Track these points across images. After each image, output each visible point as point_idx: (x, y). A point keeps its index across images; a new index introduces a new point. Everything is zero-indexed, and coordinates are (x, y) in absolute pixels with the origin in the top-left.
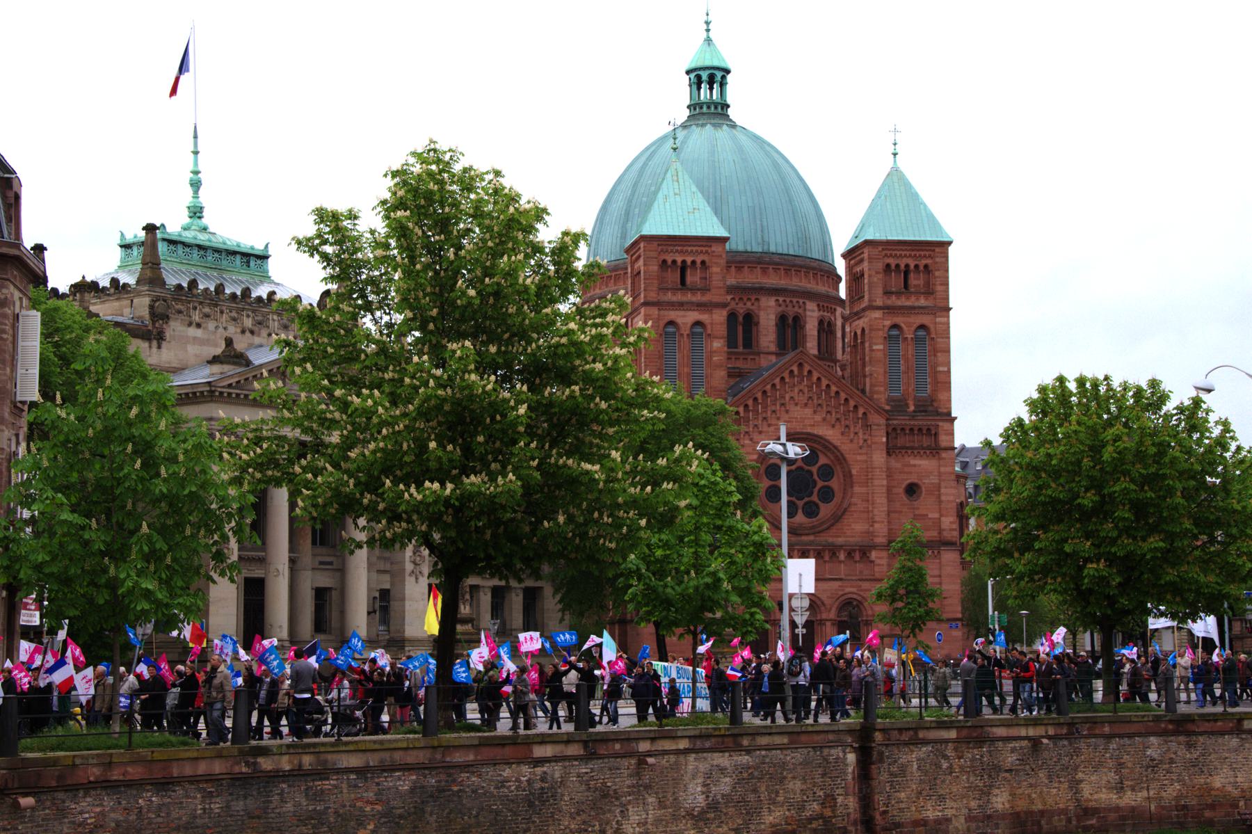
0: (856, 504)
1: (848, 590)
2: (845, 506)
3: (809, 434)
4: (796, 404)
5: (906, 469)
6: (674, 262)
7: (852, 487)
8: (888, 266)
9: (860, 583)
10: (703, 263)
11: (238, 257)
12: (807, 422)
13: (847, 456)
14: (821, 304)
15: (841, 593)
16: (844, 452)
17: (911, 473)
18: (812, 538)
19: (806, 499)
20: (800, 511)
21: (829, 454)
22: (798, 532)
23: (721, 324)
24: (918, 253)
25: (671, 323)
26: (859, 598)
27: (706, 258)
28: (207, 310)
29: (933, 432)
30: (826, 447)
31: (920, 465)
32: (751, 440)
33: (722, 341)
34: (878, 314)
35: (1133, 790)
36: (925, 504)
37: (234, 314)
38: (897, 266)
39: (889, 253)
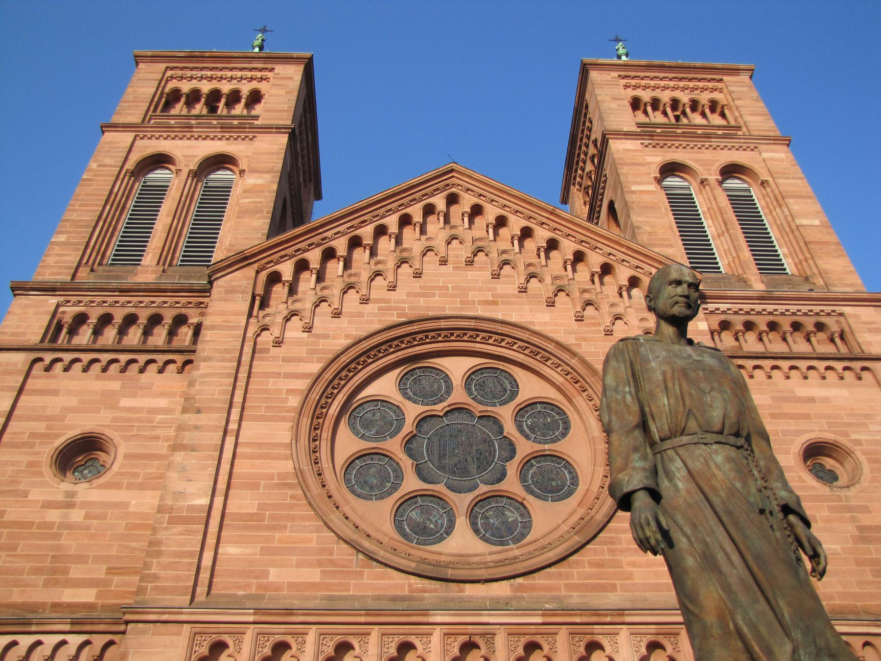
4: (444, 262)
17: (806, 417)
18: (502, 589)
20: (462, 523)
22: (450, 573)
23: (270, 153)
27: (263, 87)
30: (535, 350)
31: (826, 400)
32: (308, 329)
33: (268, 177)
39: (633, 82)
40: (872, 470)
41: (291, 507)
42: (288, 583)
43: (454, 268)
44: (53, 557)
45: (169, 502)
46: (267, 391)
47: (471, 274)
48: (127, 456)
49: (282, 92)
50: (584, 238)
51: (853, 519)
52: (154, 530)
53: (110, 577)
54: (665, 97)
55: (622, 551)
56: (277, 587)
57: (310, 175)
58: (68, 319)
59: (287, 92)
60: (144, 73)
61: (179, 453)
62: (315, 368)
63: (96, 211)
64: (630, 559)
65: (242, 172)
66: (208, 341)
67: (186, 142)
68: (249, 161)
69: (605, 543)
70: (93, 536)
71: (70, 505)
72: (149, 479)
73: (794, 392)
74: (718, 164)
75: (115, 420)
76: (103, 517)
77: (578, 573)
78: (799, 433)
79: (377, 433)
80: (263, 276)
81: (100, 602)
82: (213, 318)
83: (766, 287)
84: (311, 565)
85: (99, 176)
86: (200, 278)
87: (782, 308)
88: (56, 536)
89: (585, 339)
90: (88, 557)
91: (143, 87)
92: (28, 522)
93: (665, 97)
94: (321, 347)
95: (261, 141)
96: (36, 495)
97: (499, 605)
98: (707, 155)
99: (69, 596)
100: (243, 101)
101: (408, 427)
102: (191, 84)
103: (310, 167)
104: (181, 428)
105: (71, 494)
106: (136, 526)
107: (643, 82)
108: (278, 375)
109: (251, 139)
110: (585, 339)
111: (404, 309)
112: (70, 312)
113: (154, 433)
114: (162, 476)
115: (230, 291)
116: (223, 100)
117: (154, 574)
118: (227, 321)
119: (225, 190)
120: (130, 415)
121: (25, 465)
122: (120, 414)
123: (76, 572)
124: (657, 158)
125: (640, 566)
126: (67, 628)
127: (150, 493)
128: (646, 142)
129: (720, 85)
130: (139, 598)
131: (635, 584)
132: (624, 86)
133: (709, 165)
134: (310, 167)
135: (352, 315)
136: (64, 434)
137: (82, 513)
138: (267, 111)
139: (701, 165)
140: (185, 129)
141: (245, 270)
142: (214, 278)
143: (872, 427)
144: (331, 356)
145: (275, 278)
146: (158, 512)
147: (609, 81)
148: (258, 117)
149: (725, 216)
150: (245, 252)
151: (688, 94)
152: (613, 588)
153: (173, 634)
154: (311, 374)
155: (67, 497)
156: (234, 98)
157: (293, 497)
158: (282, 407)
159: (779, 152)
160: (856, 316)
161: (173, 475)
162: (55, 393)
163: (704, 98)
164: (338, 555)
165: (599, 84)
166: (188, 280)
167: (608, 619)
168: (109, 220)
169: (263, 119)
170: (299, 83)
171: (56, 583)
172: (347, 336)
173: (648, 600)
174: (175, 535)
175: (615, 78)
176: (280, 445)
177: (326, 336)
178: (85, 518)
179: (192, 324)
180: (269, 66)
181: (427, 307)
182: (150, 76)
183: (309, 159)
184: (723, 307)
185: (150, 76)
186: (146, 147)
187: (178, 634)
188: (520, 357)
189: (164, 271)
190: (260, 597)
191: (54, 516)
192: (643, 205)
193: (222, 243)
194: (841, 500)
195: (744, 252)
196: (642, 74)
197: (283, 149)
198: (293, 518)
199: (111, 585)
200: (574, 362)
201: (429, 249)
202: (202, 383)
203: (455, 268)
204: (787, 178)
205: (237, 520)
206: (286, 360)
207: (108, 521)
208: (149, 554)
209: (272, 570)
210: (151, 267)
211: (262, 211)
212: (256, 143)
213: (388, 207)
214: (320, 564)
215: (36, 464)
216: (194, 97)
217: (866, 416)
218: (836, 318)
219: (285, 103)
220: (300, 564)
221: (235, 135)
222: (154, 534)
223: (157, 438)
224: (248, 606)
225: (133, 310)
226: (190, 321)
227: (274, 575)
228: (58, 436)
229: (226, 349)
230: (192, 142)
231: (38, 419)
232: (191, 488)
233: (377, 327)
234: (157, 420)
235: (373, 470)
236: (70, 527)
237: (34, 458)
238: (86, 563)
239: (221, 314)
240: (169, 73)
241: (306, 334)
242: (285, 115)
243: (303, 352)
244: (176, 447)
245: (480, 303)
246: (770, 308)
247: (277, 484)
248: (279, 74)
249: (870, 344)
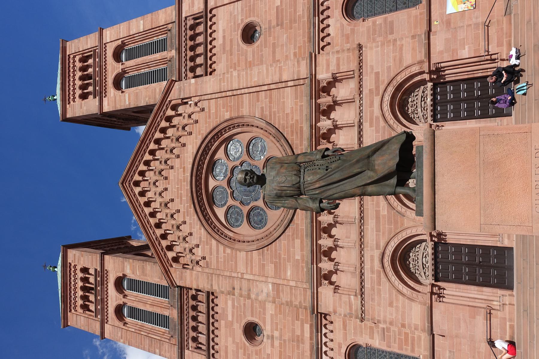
0: (262, 108)
2: (263, 124)
5: (228, 48)
7: (242, 117)
9: (365, 92)
13: (211, 128)
15: (382, 123)
16: (208, 131)
17: (231, 41)
21: (213, 148)
23: (114, 263)
25: (119, 311)
26: (391, 90)
27: (79, 268)
29: (192, 22)
31: (224, 31)
32: (198, 246)
33: (126, 263)
34: (105, 101)
39: (72, 98)
40: (254, 16)
41: (271, 251)
42: (301, 252)
43: (168, 185)
44: (293, 342)
45: (271, 299)
46: (224, 261)
47: (171, 178)
48: (252, 316)
49: (82, 259)
50: (154, 128)
51: (274, 27)
52: (282, 304)
53: (300, 319)
54: (78, 83)
55: (287, 123)
56: (302, 256)
57: (120, 242)
58: (194, 345)
59: (82, 256)
60: (73, 322)
61: (251, 296)
62: (214, 242)
63: (144, 337)
64: (290, 120)
65: (124, 276)
66: (204, 287)
67: (109, 302)
68: (118, 272)
69: (284, 129)
70: (284, 327)
71: (272, 337)
72: (261, 307)
73: (221, 44)
74: (113, 63)
75: (237, 322)
76: (277, 324)
77: (296, 141)
78: (238, 45)
79: (240, 216)
80: (174, 265)
81: (309, 322)
82: (193, 285)
83: (173, 49)
84: (294, 243)
85: (127, 338)
86: (175, 291)
87: (183, 44)
88: (285, 341)
89: (200, 132)
90: (292, 328)
91: (81, 322)
92: (279, 353)
93: (78, 83)
94: (205, 240)
95: (108, 268)
96: (269, 351)
98: (109, 68)
99: (307, 334)
100: (87, 276)
101: (237, 204)
102: (78, 300)
103: (116, 242)
104: (241, 295)
105: (268, 338)
106: (280, 310)
107: (72, 93)
108: (217, 257)
109: (107, 272)
110: (200, 132)
111: (187, 206)
112: (191, 344)
113: (242, 306)
114: (260, 302)
115: (181, 278)
116: (87, 285)
117: (299, 303)
118: (195, 279)
119: (131, 281)
120: (235, 316)
121: (257, 356)
122: (235, 320)
124: (111, 91)
125: (293, 116)
126: (319, 334)
127: (267, 306)
128: (104, 95)
129: (72, 56)
130: (308, 309)
131: (300, 119)
132: (74, 102)
133: (114, 68)
134: (116, 242)
135: (191, 228)
136: (244, 342)
137: (275, 332)
138: (92, 265)
139: (114, 72)
140: (103, 302)
141: (171, 272)
142: (175, 285)
143: (236, 13)
144: (209, 236)
145: (176, 260)
146: (275, 303)
147: (71, 109)
148: (95, 269)
149: (140, 64)
150: (163, 272)
151: (77, 72)
152: (301, 128)
153: (321, 295)
154: (217, 243)
155: (269, 339)
156: (85, 280)
157: (268, 251)
158: (231, 255)
159: (106, 34)
160: (186, 12)
161: (260, 298)
162: (226, 347)
163: (78, 65)
164: (290, 233)
165: (73, 113)
166: (176, 296)
167: (314, 131)
168: (148, 332)
169: (97, 266)
170: (77, 251)
171: (302, 339)
172: (200, 229)
173: (306, 115)
174: (284, 296)
175: (70, 106)
176: (247, 256)
177: (200, 238)
178: (277, 331)
179: (196, 293)
180: (68, 265)
181: (187, 196)
182: (75, 319)
183: (113, 243)
184: (183, 70)
185: (75, 319)
186: (112, 319)
187: (321, 293)
188: (208, 158)
189: (171, 306)
190: (307, 262)
191: (277, 343)
192: (135, 100)
193: (158, 282)
194: (266, 31)
195: (157, 57)
196: (67, 93)
197: (112, 258)
198: (276, 250)
199: (303, 319)
200: (210, 137)
201: (160, 194)
202: (222, 288)
203: (169, 184)
204: (120, 32)
205: (277, 272)
206: (211, 254)
207: (278, 322)
208: (292, 305)
209: (296, 258)
210: (170, 311)
211: (143, 266)
212: (109, 269)
213: (141, 212)
214: (293, 240)
215: (256, 351)
216: (85, 298)
217: (231, 15)
218: (187, 21)
219: (88, 257)
220: (294, 247)
221: (105, 279)
222: (284, 304)
223: (244, 304)
224: (310, 267)
225: (190, 318)
226: (194, 294)
227: (298, 257)
228: (244, 344)
229: (207, 279)
230: (109, 298)
231: (238, 352)
232: (265, 291)
233: (196, 217)
234: (237, 305)
235: (256, 218)
236: (281, 336)
237: (254, 353)
238: (295, 328)
239: (192, 282)
240: (73, 311)
241: (200, 246)
242: (94, 257)
243: (207, 247)
244: (249, 297)
245: (184, 174)
246: (184, 50)
247: (262, 257)
248: (72, 261)
249: (199, 8)
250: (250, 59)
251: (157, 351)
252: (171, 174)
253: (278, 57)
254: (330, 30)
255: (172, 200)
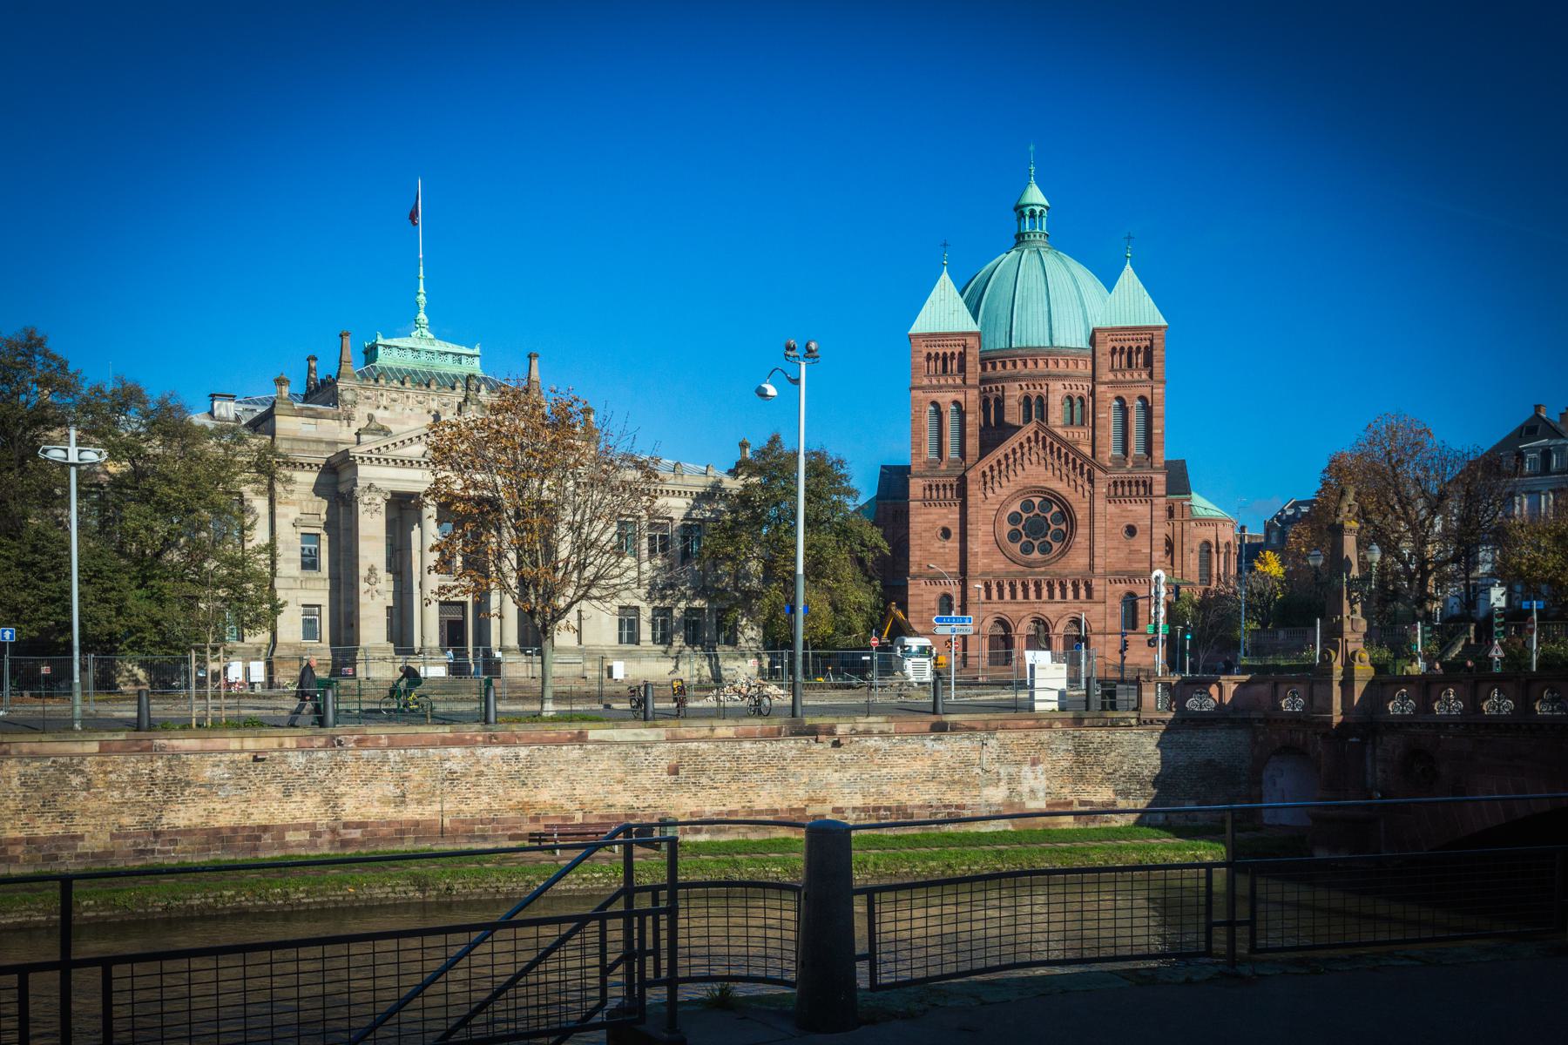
1: (1070, 611)
3: (1042, 487)
5: (1124, 514)
6: (937, 354)
8: (1114, 349)
10: (960, 353)
11: (450, 356)
12: (1041, 478)
13: (1074, 505)
14: (1066, 383)
19: (1042, 540)
24: (1139, 337)
28: (394, 395)
29: (1148, 483)
35: (419, 802)
36: (1141, 542)
37: (420, 398)
38: (1122, 348)
39: (1114, 337)
97: (1042, 573)
123: (951, 564)
124: (1111, 395)
162: (931, 514)
191: (941, 550)
227: (995, 566)
243: (994, 501)
250: (1114, 531)
251: (914, 451)
252: (1042, 468)
253: (1111, 551)
254: (1119, 585)
255: (1023, 469)
